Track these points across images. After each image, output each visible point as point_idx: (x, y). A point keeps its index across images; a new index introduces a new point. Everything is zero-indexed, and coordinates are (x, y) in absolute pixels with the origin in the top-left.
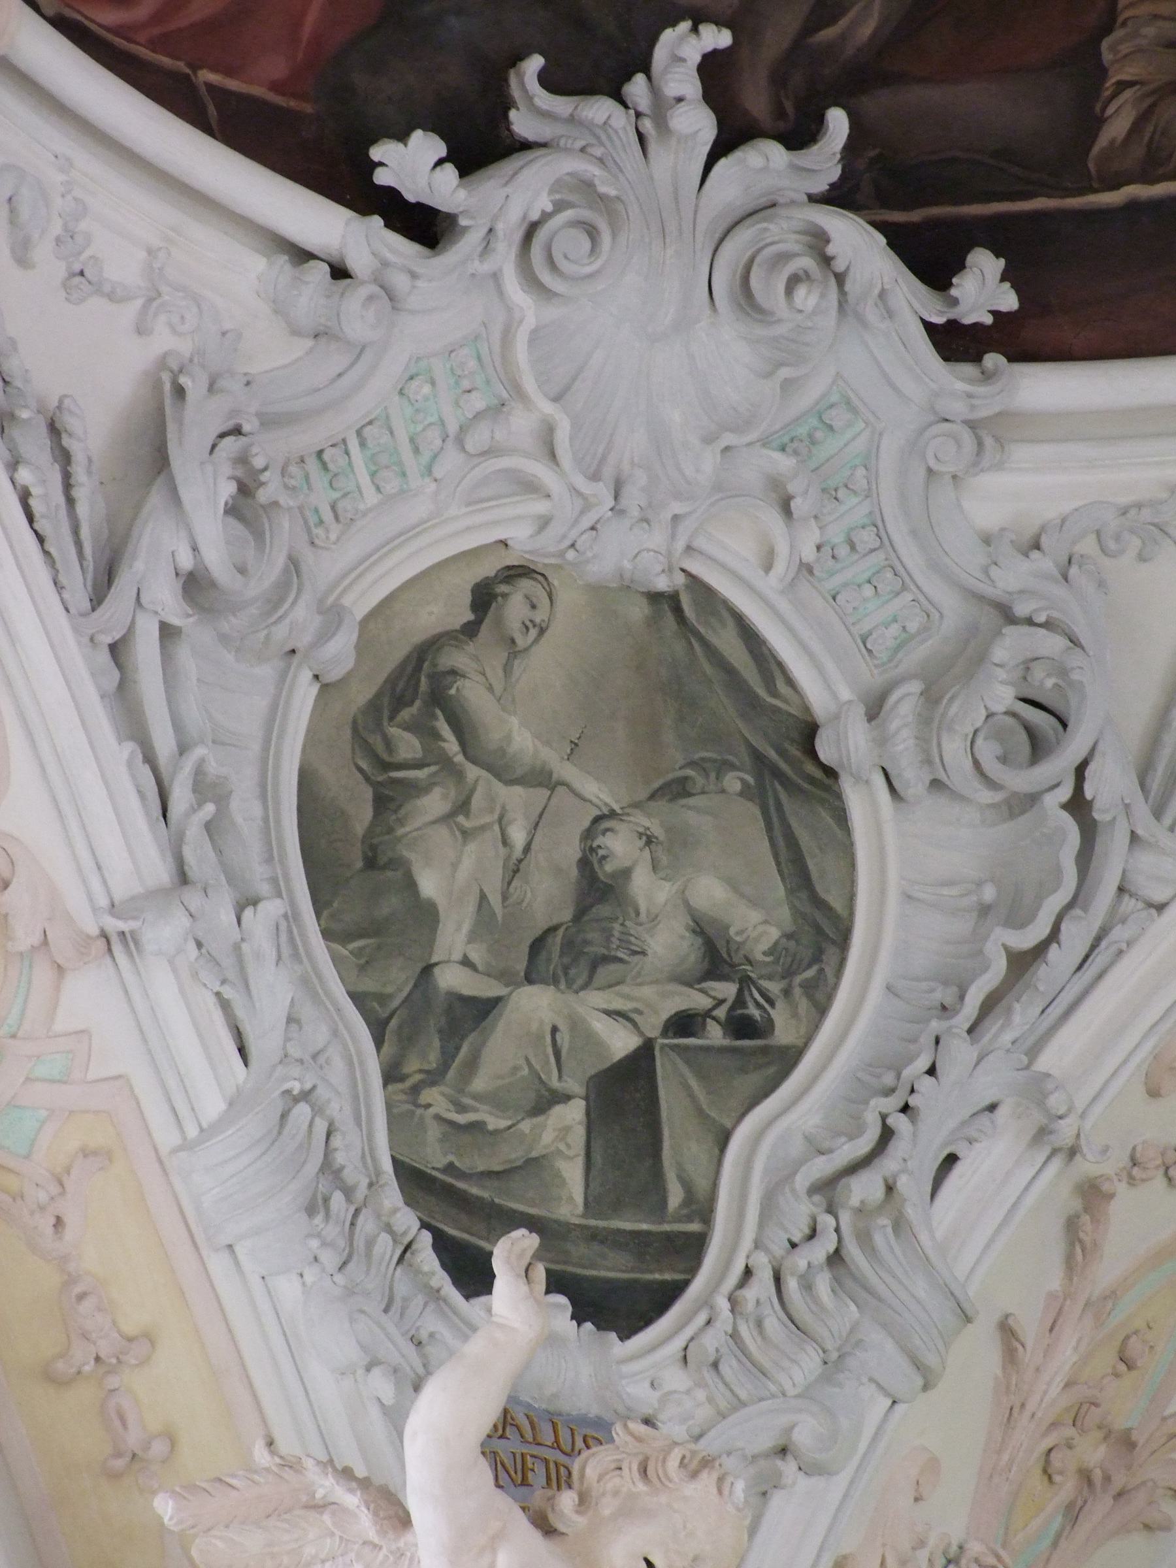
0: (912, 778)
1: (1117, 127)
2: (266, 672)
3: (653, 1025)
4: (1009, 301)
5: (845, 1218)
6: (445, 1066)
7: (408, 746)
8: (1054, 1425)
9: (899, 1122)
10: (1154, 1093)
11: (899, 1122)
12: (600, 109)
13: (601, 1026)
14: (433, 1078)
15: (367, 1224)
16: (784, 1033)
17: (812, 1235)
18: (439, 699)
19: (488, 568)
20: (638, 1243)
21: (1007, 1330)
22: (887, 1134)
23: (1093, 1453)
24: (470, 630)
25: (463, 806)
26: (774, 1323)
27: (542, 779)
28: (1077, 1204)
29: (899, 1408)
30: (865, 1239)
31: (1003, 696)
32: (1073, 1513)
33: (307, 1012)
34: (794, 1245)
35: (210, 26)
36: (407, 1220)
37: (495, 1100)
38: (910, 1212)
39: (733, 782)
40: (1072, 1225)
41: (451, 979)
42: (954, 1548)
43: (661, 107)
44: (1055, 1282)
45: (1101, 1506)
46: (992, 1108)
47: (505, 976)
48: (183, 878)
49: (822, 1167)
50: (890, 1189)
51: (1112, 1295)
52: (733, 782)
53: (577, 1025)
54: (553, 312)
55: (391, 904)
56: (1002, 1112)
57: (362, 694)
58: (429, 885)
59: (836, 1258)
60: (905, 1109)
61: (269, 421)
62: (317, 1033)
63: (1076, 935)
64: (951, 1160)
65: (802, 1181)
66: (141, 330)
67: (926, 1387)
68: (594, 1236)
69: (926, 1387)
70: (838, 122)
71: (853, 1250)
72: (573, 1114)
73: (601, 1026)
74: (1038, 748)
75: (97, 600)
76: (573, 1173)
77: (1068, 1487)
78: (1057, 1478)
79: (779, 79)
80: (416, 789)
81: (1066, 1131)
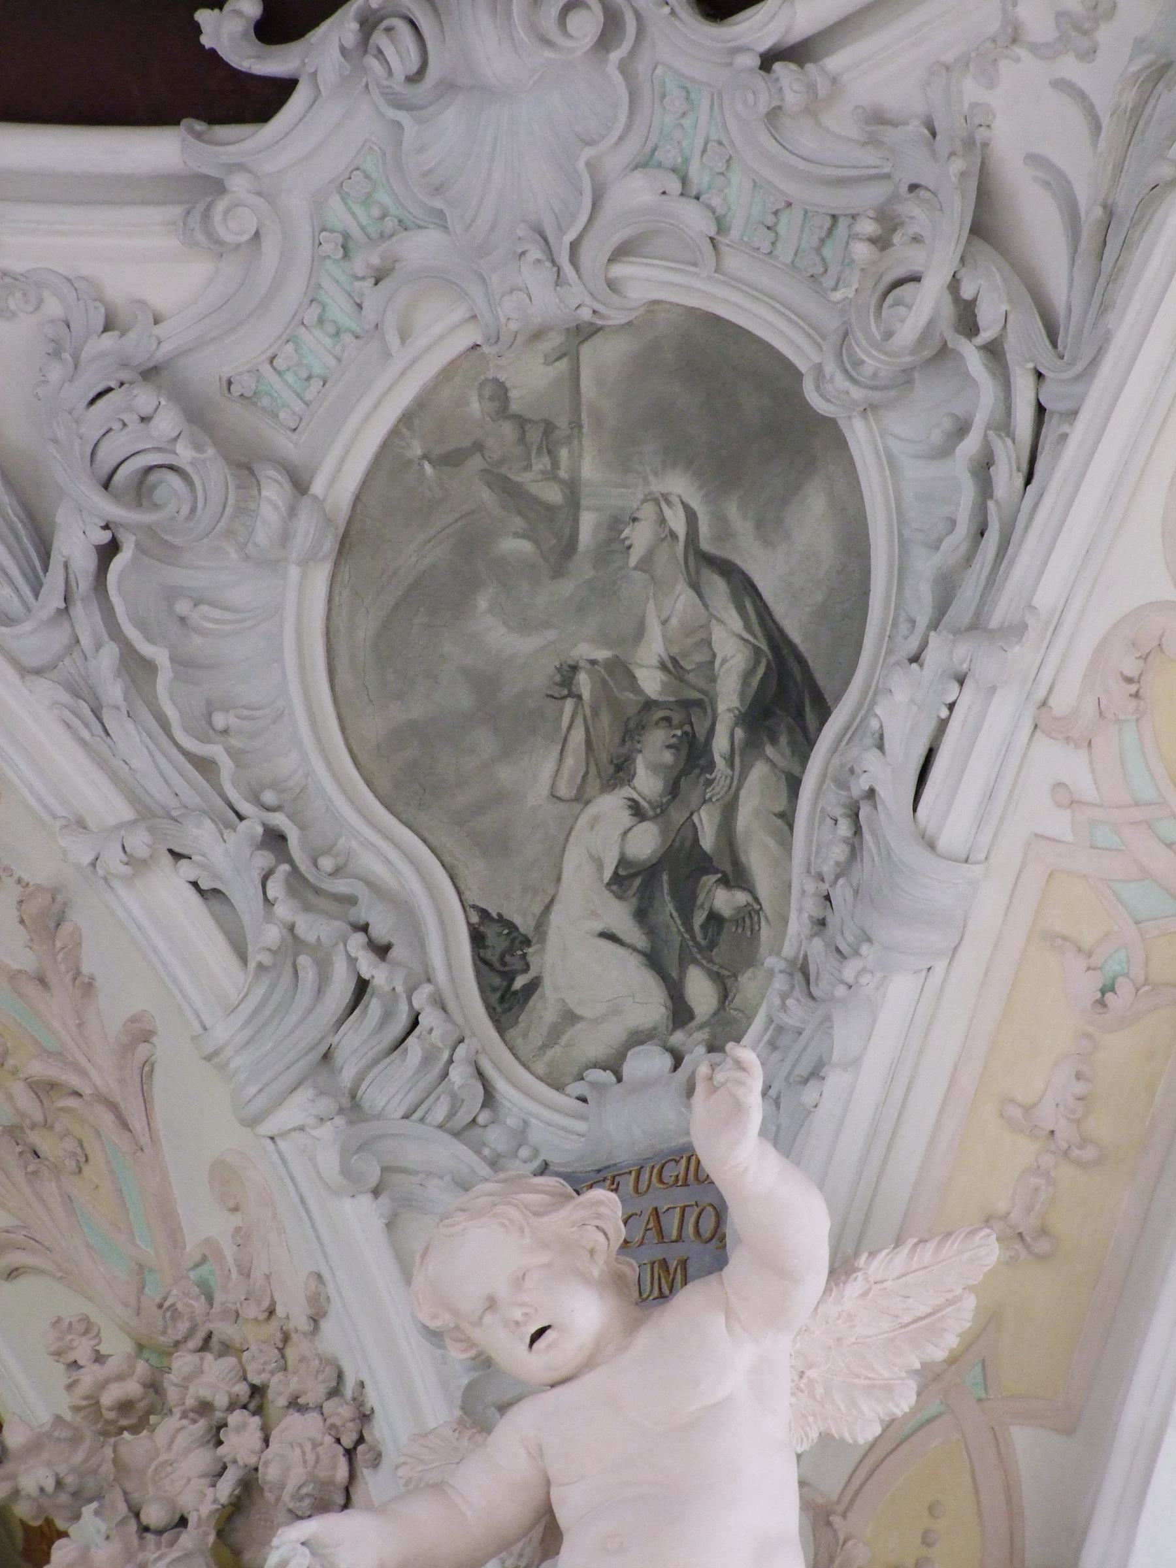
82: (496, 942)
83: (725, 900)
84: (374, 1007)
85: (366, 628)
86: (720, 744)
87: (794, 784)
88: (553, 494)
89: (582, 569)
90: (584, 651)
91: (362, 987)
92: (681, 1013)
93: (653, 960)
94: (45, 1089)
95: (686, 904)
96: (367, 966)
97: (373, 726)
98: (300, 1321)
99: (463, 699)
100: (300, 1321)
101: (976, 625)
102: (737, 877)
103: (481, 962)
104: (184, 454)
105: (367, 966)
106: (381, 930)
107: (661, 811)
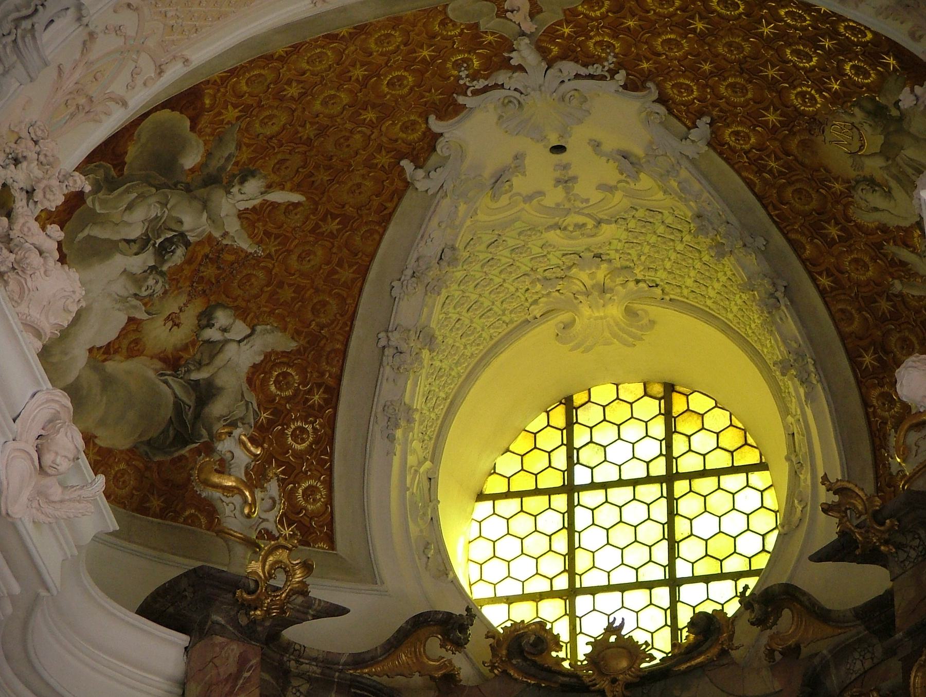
5: (19, 31)
8: (71, 93)
9: (40, 8)
10: (115, 11)
11: (40, 8)
17: (9, 34)
21: (60, 69)
22: (36, 11)
23: (82, 101)
28: (87, 38)
29: (22, 86)
30: (23, 37)
32: (73, 115)
34: (4, 35)
38: (37, 34)
40: (84, 43)
42: (34, 121)
44: (77, 56)
46: (68, 9)
49: (16, 15)
50: (33, 25)
51: (92, 63)
56: (69, 12)
59: (15, 41)
60: (42, 5)
64: (52, 21)
65: (11, 18)
67: (31, 81)
69: (31, 81)
71: (19, 41)
77: (72, 109)
78: (69, 107)
81: (85, 20)
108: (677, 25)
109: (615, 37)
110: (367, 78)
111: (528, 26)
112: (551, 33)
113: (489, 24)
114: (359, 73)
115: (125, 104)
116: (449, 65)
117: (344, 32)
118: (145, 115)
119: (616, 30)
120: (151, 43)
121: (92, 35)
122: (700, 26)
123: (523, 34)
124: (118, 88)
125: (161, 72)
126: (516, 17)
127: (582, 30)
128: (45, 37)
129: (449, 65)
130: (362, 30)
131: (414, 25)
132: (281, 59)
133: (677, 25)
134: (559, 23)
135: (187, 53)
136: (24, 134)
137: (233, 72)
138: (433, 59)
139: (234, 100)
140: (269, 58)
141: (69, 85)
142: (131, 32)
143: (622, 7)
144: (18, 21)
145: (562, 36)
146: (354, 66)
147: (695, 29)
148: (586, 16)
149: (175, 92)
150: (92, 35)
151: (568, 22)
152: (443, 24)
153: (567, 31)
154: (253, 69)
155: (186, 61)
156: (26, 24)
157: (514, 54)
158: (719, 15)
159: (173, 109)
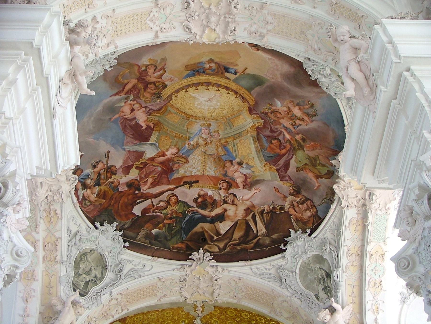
0: (112, 271)
1: (138, 238)
2: (77, 250)
3: (90, 280)
4: (128, 246)
6: (78, 277)
7: (83, 258)
12: (109, 225)
13: (87, 278)
14: (77, 278)
15: (69, 285)
16: (98, 283)
18: (86, 255)
19: (92, 249)
20: (84, 292)
22: (101, 291)
23: (105, 314)
24: (89, 252)
25: (85, 262)
26: (90, 300)
27: (90, 262)
30: (98, 297)
31: (119, 268)
32: (103, 317)
33: (71, 271)
35: (89, 212)
36: (72, 286)
37: (79, 280)
39: (101, 267)
41: (80, 272)
43: (113, 226)
45: (105, 317)
47: (83, 273)
48: (67, 261)
51: (110, 306)
52: (101, 267)
53: (86, 278)
54: (102, 236)
55: (78, 266)
57: (82, 254)
58: (81, 266)
59: (96, 297)
61: (83, 236)
62: (71, 272)
63: (117, 284)
66: (78, 228)
68: (82, 291)
70: (123, 231)
72: (84, 283)
73: (87, 278)
74: (119, 272)
75: (69, 242)
76: (82, 286)
77: (103, 315)
79: (120, 228)
80: (82, 260)
82: (316, 295)
83: (329, 289)
84: (310, 302)
85: (302, 279)
86: (325, 279)
87: (330, 280)
88: (311, 268)
89: (314, 272)
90: (315, 276)
91: (309, 301)
92: (329, 296)
93: (326, 294)
94: (293, 313)
95: (327, 290)
96: (309, 300)
97: (305, 285)
98: (312, 322)
99: (310, 282)
100: (312, 322)
101: (338, 267)
102: (329, 287)
103: (316, 297)
104: (288, 273)
105: (309, 300)
106: (309, 297)
107: (323, 284)
108: (233, 319)
109: (219, 320)
110: (162, 322)
111: (200, 315)
112: (205, 317)
113: (192, 313)
114: (161, 320)
115: (113, 317)
116: (180, 321)
117: (160, 310)
118: (114, 322)
119: (219, 318)
120: (122, 304)
121: (112, 299)
122: (238, 319)
123: (199, 316)
124: (113, 313)
125: (122, 311)
126: (198, 312)
127: (212, 317)
128: (103, 297)
129: (180, 321)
130: (164, 310)
131: (175, 310)
132: (145, 314)
133: (233, 319)
134: (207, 315)
135: (128, 308)
136: (93, 319)
137: (134, 315)
138: (178, 319)
139: (133, 322)
140: (143, 313)
141: (104, 310)
142: (119, 300)
143: (222, 313)
144: (97, 293)
145: (207, 318)
146: (160, 318)
147: (237, 320)
148: (213, 314)
149: (121, 318)
150: (112, 299)
151: (209, 315)
152: (182, 311)
153: (208, 317)
154: (139, 315)
155: (128, 309)
156: (99, 294)
157: (195, 321)
158: (243, 318)
159: (120, 322)
